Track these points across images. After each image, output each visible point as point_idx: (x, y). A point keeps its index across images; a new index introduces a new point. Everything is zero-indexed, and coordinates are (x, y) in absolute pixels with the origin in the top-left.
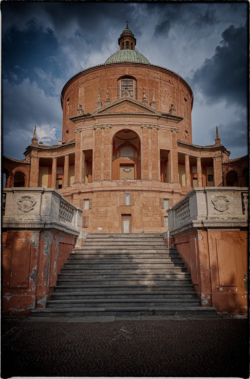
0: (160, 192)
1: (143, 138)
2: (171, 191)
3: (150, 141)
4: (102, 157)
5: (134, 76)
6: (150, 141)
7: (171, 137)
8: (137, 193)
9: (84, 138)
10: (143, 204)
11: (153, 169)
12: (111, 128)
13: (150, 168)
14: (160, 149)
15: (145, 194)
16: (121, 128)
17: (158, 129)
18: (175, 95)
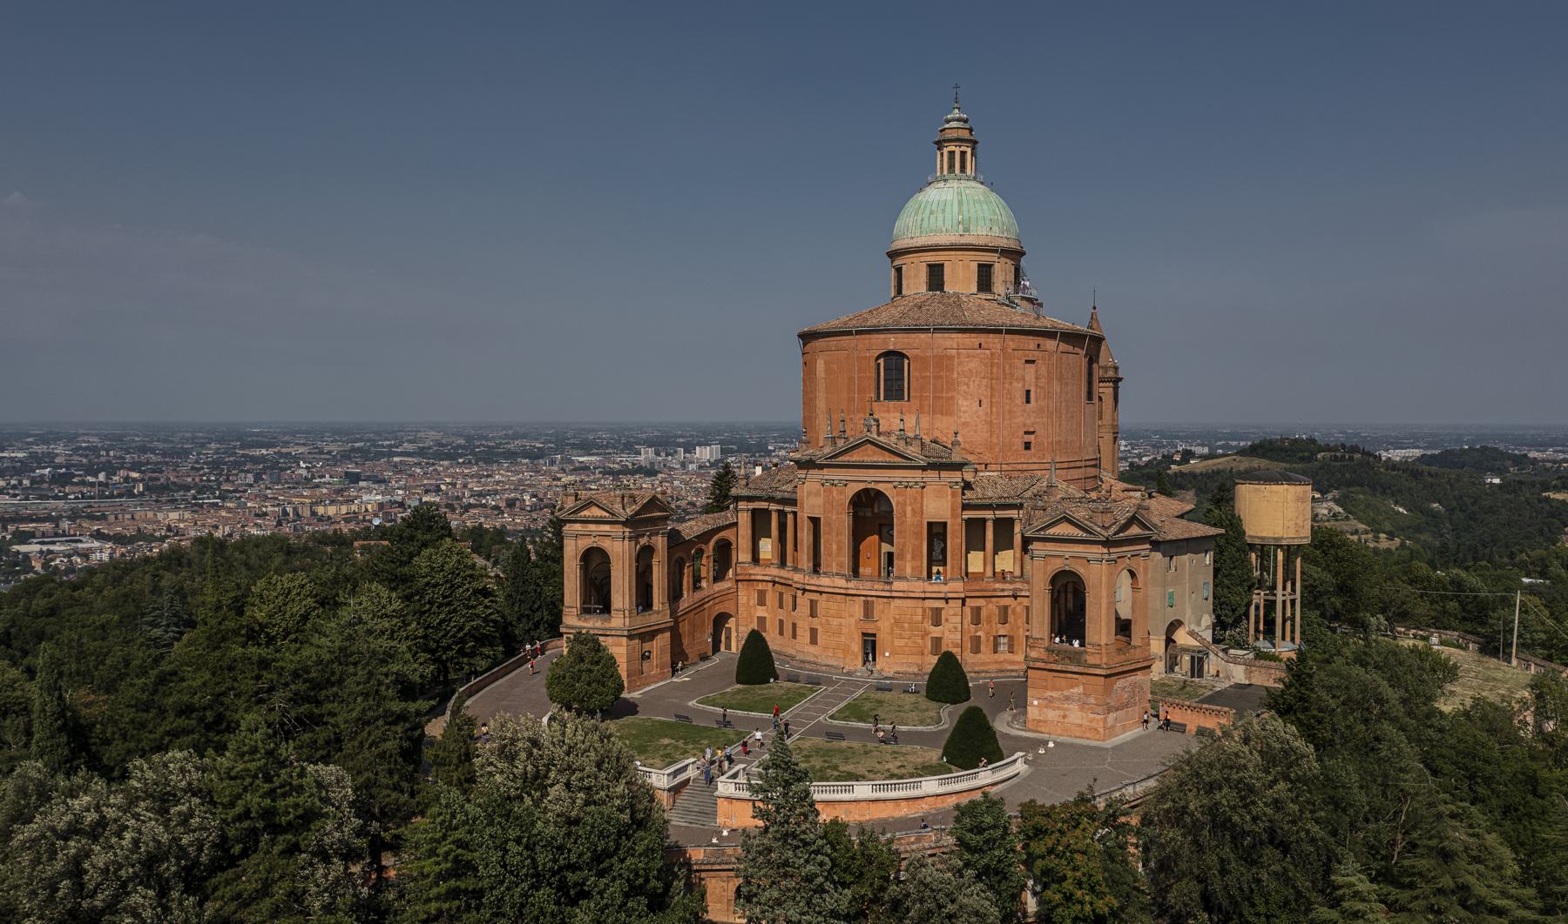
0: (924, 599)
1: (898, 503)
2: (942, 595)
3: (909, 509)
4: (834, 534)
5: (904, 352)
6: (909, 509)
7: (949, 497)
8: (885, 600)
9: (809, 494)
10: (895, 618)
11: (913, 558)
12: (846, 485)
13: (909, 557)
14: (930, 524)
15: (898, 602)
16: (862, 486)
18: (995, 370)
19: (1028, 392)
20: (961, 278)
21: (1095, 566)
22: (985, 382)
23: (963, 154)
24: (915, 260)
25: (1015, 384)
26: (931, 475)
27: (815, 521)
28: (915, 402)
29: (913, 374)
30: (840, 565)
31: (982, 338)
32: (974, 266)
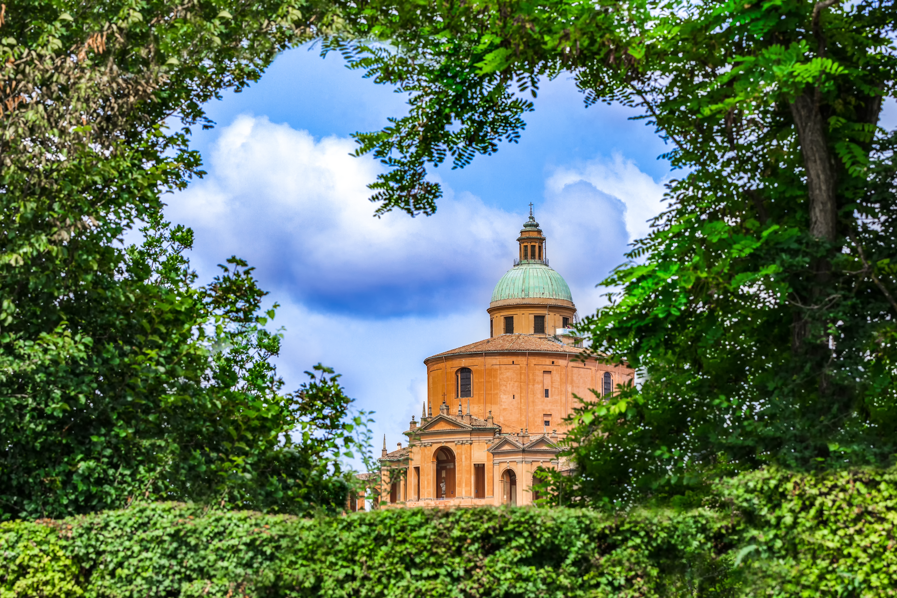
11: (466, 486)
13: (464, 485)
17: (471, 444)
19: (547, 391)
20: (524, 323)
21: (520, 465)
22: (516, 384)
23: (533, 247)
24: (498, 315)
25: (536, 385)
26: (475, 438)
27: (417, 469)
28: (476, 397)
29: (474, 378)
30: (429, 494)
31: (514, 359)
32: (532, 317)
